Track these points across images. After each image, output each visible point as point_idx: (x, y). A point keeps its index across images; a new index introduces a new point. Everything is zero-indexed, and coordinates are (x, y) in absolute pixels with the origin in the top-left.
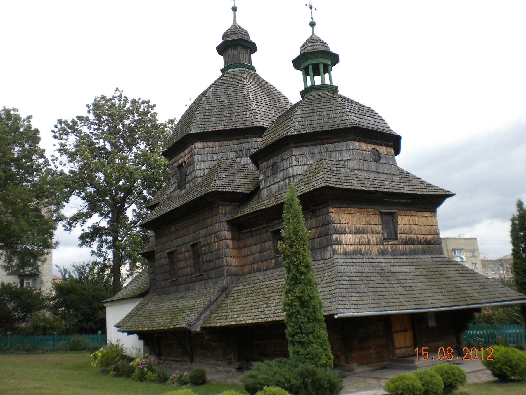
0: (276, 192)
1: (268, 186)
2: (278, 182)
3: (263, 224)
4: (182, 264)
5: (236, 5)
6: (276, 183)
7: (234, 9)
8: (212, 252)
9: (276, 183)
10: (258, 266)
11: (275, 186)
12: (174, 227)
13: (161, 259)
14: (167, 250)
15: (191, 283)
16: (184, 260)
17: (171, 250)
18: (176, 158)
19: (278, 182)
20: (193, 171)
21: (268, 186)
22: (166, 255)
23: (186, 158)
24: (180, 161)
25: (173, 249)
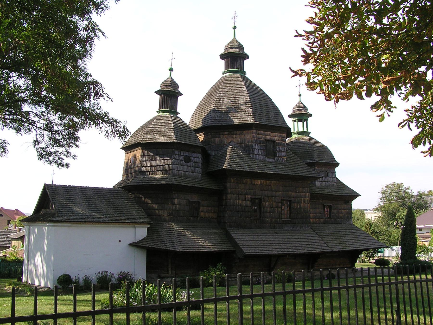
0: (326, 186)
1: (321, 181)
2: (327, 182)
3: (320, 200)
4: (269, 210)
5: (235, 25)
6: (326, 182)
7: (235, 28)
8: (300, 208)
9: (326, 182)
10: (313, 221)
11: (325, 183)
12: (259, 181)
13: (239, 200)
14: (248, 195)
15: (277, 224)
16: (271, 207)
17: (254, 197)
18: (263, 132)
19: (327, 182)
20: (283, 152)
21: (321, 181)
22: (250, 199)
23: (276, 138)
24: (268, 138)
25: (257, 197)
